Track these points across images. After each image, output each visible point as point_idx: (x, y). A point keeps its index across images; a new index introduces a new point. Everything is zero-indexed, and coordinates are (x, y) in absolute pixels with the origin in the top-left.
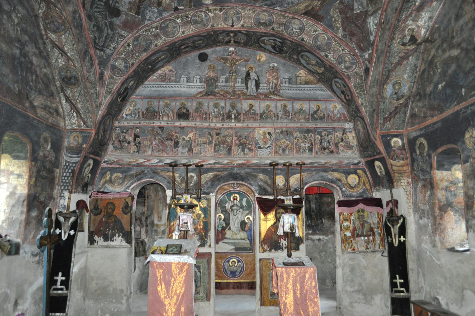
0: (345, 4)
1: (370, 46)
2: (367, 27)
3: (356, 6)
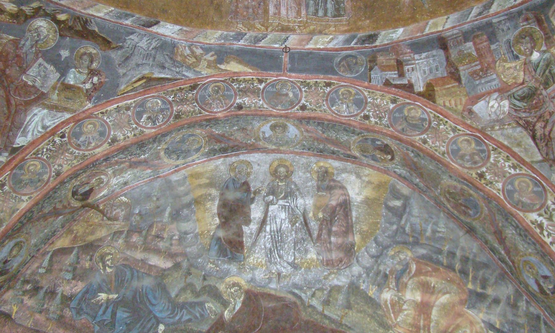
0: (19, 52)
1: (6, 150)
2: (26, 116)
3: (33, 71)
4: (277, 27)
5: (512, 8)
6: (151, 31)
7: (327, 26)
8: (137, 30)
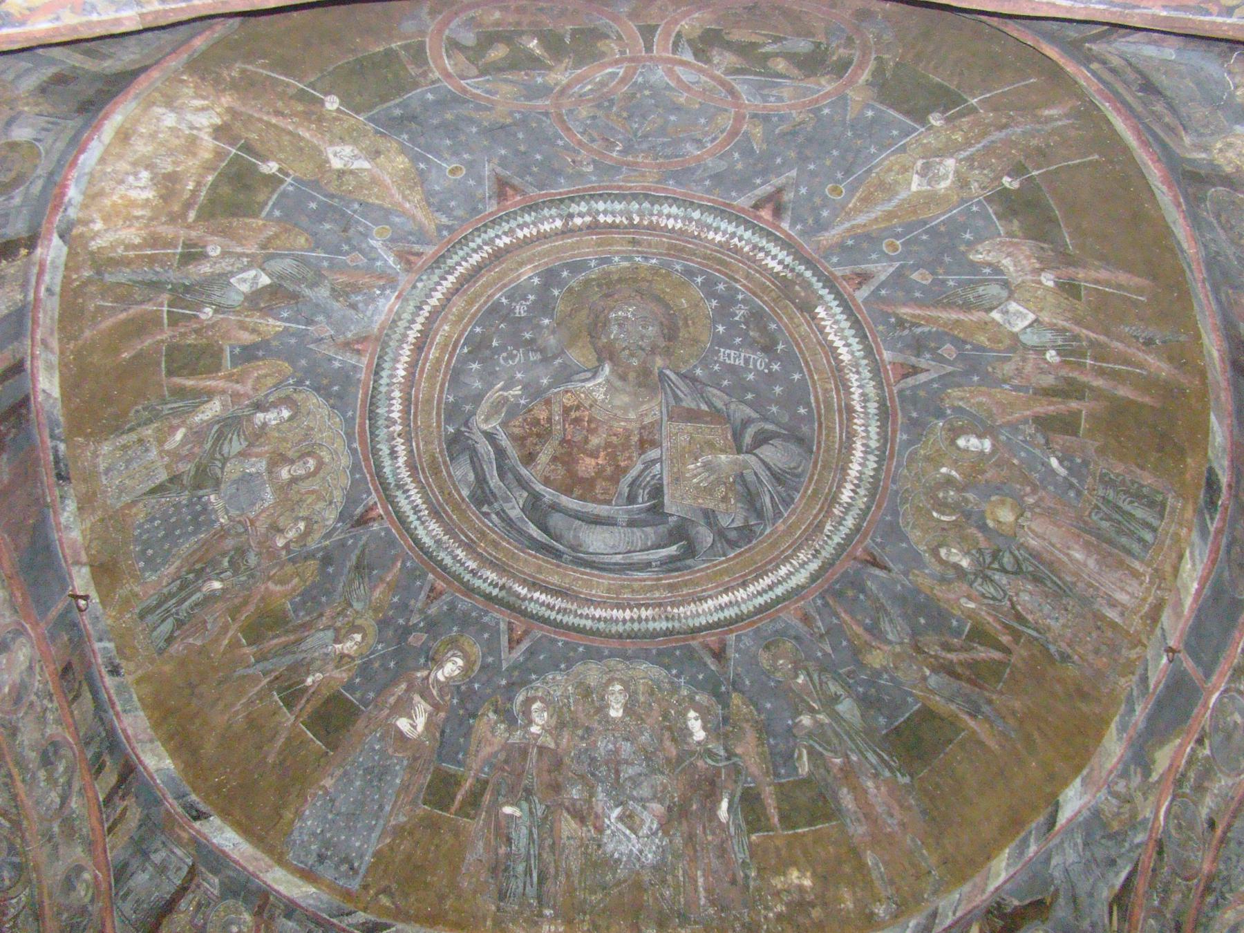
4: (1145, 625)
5: (1178, 205)
6: (1062, 827)
7: (1176, 539)
8: (1051, 844)
